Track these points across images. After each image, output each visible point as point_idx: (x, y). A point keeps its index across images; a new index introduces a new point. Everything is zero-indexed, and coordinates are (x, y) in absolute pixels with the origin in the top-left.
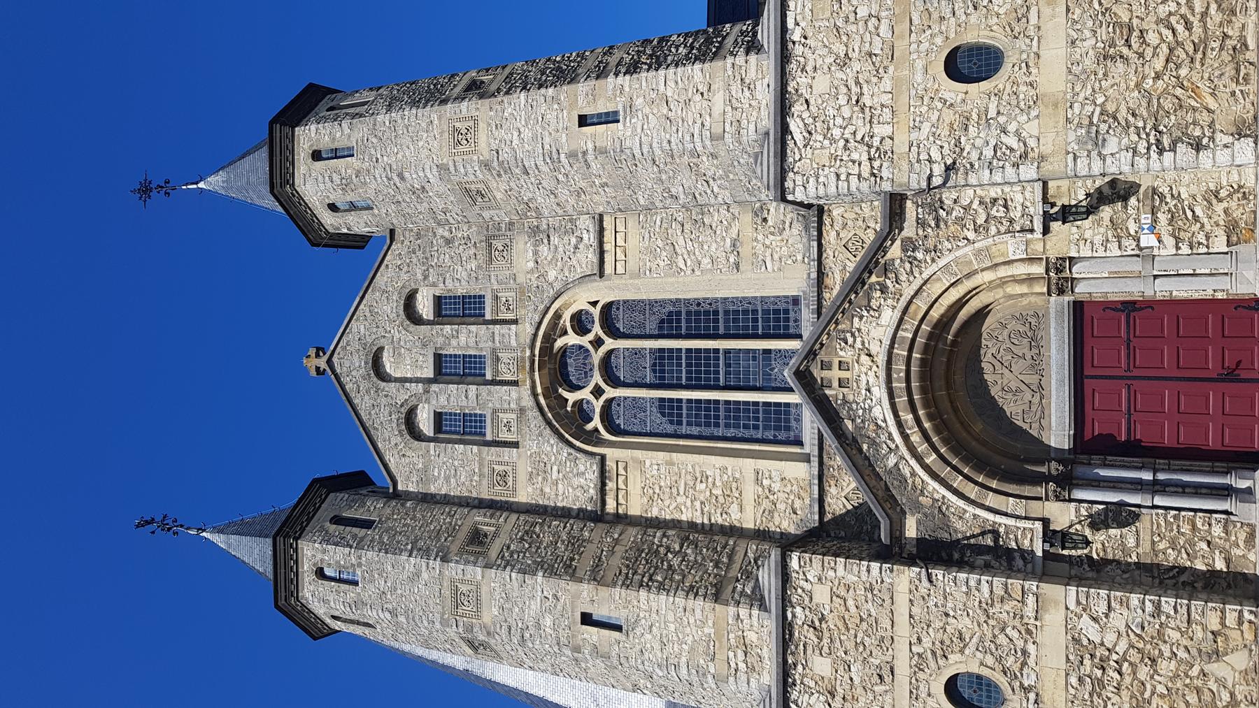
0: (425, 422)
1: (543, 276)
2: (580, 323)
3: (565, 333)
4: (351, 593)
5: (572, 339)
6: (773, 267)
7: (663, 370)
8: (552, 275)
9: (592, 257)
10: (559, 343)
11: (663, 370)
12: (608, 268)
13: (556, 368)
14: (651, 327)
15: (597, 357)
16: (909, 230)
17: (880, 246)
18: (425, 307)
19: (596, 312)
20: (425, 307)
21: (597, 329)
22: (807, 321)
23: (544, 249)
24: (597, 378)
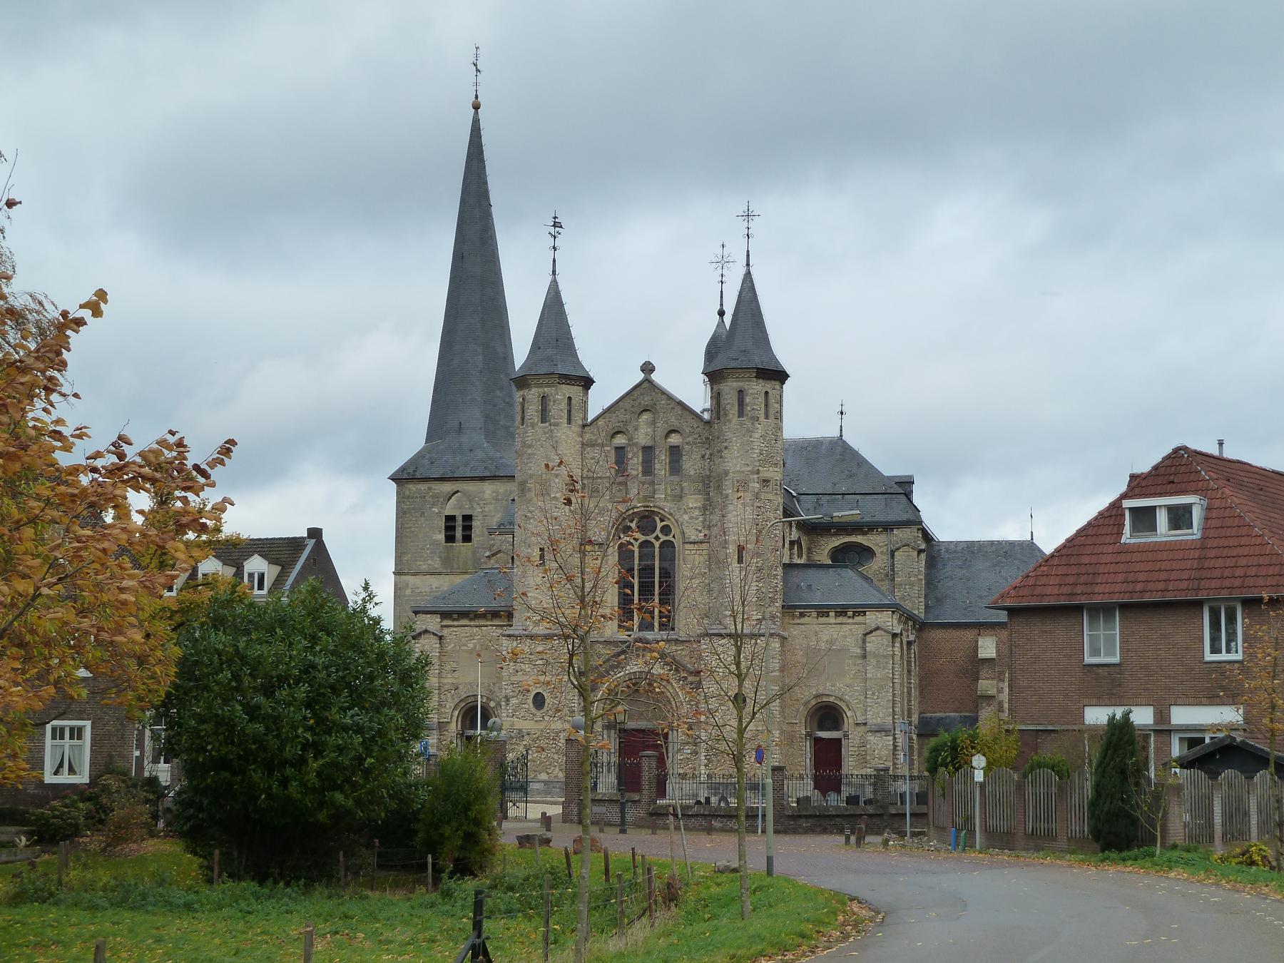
0: (620, 440)
1: (686, 513)
2: (667, 530)
3: (662, 520)
4: (536, 419)
5: (660, 525)
6: (687, 623)
7: (647, 571)
8: (686, 517)
9: (693, 538)
10: (657, 519)
11: (647, 571)
12: (688, 546)
13: (647, 520)
14: (666, 565)
15: (651, 538)
16: (690, 679)
17: (685, 669)
18: (674, 439)
19: (670, 538)
20: (674, 439)
21: (663, 538)
22: (664, 634)
23: (697, 513)
24: (642, 538)
